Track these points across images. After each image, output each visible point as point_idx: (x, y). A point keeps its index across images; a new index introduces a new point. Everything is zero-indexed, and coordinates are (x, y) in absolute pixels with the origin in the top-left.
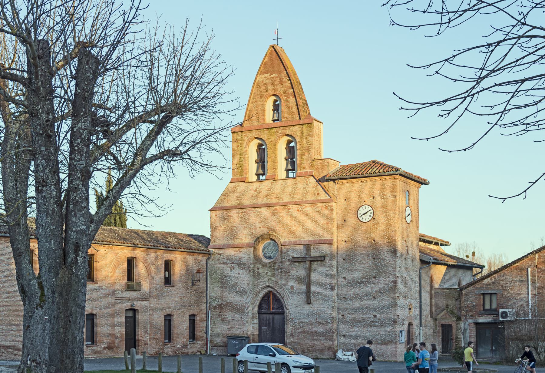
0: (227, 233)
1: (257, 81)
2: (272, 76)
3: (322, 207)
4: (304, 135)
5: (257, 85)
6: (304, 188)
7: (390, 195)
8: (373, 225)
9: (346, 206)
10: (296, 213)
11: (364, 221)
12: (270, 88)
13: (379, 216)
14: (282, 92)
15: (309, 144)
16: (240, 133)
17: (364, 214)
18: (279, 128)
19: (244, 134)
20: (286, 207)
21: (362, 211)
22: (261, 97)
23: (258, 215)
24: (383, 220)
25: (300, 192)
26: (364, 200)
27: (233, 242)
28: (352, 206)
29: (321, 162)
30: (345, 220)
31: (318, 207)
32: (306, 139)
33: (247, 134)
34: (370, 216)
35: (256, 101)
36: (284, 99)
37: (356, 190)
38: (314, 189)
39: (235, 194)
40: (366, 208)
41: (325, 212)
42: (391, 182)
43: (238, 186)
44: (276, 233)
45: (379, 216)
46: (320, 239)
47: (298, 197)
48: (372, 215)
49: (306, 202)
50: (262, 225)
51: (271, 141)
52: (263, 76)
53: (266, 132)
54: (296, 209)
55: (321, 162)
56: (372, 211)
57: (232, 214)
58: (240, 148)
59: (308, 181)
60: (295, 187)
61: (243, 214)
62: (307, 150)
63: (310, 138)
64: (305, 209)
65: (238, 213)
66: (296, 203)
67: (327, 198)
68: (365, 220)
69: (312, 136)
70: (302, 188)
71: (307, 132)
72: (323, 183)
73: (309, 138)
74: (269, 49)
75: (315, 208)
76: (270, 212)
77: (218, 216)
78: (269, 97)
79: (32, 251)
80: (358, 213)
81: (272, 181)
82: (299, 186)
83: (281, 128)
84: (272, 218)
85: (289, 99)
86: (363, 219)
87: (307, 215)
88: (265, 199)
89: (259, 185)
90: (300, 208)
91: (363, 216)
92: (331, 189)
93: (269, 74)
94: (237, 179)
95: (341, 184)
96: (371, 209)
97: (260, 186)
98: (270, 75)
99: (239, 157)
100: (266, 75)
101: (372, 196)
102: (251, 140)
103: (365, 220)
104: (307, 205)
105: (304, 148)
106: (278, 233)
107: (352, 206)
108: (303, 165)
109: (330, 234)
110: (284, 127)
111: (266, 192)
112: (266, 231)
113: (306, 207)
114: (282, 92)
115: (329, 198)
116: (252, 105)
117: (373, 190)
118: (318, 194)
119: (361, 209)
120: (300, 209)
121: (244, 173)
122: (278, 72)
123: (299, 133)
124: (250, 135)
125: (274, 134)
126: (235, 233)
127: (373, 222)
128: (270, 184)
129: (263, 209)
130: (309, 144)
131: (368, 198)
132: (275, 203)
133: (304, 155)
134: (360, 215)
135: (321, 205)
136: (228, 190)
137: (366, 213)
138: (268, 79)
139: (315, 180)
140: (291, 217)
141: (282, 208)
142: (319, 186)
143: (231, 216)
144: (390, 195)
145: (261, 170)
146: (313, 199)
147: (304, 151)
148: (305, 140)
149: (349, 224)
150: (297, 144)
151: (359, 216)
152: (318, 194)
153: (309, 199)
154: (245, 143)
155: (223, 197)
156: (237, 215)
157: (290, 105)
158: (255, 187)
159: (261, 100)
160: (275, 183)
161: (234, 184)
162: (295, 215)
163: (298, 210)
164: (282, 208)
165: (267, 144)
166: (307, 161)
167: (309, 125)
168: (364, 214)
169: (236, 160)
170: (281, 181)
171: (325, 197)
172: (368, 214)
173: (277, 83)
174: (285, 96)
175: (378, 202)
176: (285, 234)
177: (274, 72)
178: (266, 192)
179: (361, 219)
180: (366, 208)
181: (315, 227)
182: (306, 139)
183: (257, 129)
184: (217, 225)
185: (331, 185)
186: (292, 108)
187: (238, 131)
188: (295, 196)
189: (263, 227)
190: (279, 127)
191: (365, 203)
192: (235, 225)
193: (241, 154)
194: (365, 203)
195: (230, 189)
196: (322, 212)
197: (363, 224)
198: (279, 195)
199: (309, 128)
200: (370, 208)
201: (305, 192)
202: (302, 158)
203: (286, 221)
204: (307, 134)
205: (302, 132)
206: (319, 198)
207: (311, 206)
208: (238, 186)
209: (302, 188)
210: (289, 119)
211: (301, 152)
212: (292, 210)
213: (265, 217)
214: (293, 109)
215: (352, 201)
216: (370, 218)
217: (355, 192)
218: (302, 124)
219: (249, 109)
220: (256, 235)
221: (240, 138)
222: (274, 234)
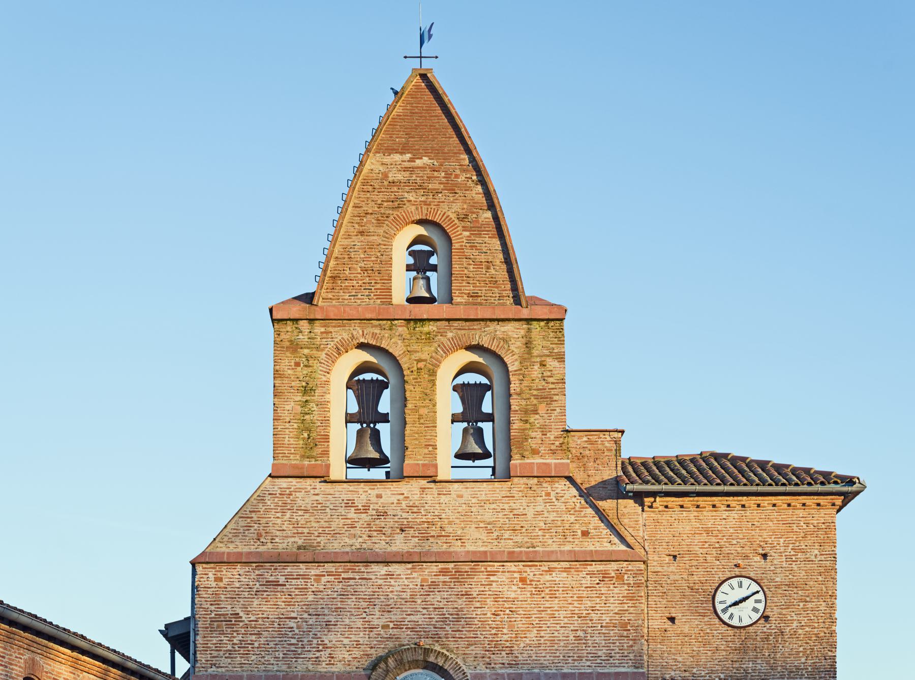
0: (262, 640)
1: (365, 170)
2: (418, 162)
3: (605, 576)
4: (535, 352)
5: (363, 184)
6: (539, 513)
7: (816, 552)
8: (762, 635)
9: (677, 577)
10: (515, 588)
11: (735, 622)
12: (411, 197)
13: (784, 612)
14: (453, 216)
15: (551, 380)
16: (304, 325)
17: (736, 604)
18: (446, 323)
19: (319, 329)
20: (481, 567)
21: (728, 594)
22: (379, 223)
23: (380, 587)
24: (795, 624)
25: (522, 524)
26: (735, 562)
27: (284, 668)
28: (695, 578)
29: (593, 438)
30: (672, 620)
31: (591, 574)
32: (543, 365)
33: (331, 329)
34: (755, 610)
35: (362, 233)
36: (460, 237)
37: (708, 532)
38: (572, 519)
39: (288, 515)
40: (740, 586)
41: (616, 591)
42: (820, 516)
43: (299, 490)
44: (443, 646)
45: (784, 612)
46: (600, 670)
47: (519, 539)
48: (761, 606)
49: (549, 558)
50: (394, 618)
51: (419, 361)
52: (387, 159)
53: (402, 330)
54: (516, 575)
55: (593, 438)
56: (760, 596)
57: (282, 580)
58: (301, 371)
59: (553, 494)
60: (506, 506)
61: (324, 579)
62: (547, 398)
63: (556, 363)
64: (548, 577)
65: (305, 577)
66: (513, 558)
67: (614, 548)
68: (740, 620)
69: (561, 358)
70: (530, 512)
71: (545, 343)
72: (598, 502)
73: (552, 363)
74: (408, 81)
75: (583, 574)
76: (423, 580)
77: (225, 581)
78: (407, 224)
79: (377, 379)
80: (718, 599)
81: (423, 482)
82: (520, 504)
83: (456, 324)
84: (429, 598)
85: (479, 240)
86: (731, 617)
87: (553, 596)
88: (399, 538)
89: (376, 492)
90: (530, 573)
91: (731, 610)
92: (625, 521)
93: (408, 156)
94: (295, 467)
95: (661, 508)
96: (758, 588)
97: (379, 496)
98: (412, 160)
99: (299, 398)
100: (397, 157)
101: (761, 552)
102: (341, 350)
103: (740, 620)
104: (555, 565)
105: (535, 393)
106: (452, 645)
107: (695, 578)
108: (532, 443)
109: (631, 656)
110: (466, 320)
111: (405, 515)
112: (406, 637)
113: (550, 570)
114: (453, 216)
115: (623, 547)
116: (346, 242)
117: (765, 534)
118: (585, 534)
119: (725, 587)
120: (531, 577)
121: (317, 451)
122: (435, 153)
123: (517, 346)
124: (341, 334)
125: (429, 338)
126: (293, 641)
127: (762, 627)
128: (417, 491)
129: (395, 568)
130: (551, 380)
131: (746, 557)
132: (438, 553)
133: (535, 412)
134: (724, 606)
135: (601, 567)
136: (261, 499)
137: (745, 599)
138: (406, 169)
139: (574, 492)
140: (496, 598)
141: (467, 568)
142: (590, 511)
143: (276, 584)
144: (816, 552)
145: (371, 448)
146: (568, 548)
147: (535, 402)
148: (536, 367)
149: (686, 630)
150: (512, 378)
151: (719, 607)
152: (585, 534)
153: (554, 547)
154: (323, 355)
155: (242, 523)
156: (301, 582)
157: (483, 258)
158: (364, 497)
159: (381, 231)
160: (435, 492)
161: (283, 483)
162: (513, 595)
163: (523, 580)
164: (467, 568)
165: (405, 366)
166: (544, 430)
167: (551, 324)
168: (736, 604)
169: (287, 407)
170: (456, 485)
171: (606, 543)
172: (750, 603)
173: (437, 186)
174: (465, 229)
175: (779, 570)
176: (478, 650)
177: (426, 154)
178: (405, 515)
179: (725, 617)
180: (740, 586)
181: (580, 633)
182: (543, 365)
183: (368, 316)
184: (223, 611)
185: (625, 510)
186: (488, 268)
187: (297, 316)
188: (506, 536)
189: (397, 627)
190: (448, 320)
191: (737, 571)
192: (293, 615)
193: (307, 390)
194: (737, 571)
195: (268, 497)
196: (604, 590)
197: (731, 632)
198: (449, 529)
199: (552, 335)
200: (755, 587)
201: (542, 524)
202: (526, 421)
203: (479, 611)
204: (546, 352)
205: (528, 344)
206: (590, 546)
207: (566, 570)
208: (299, 490)
209: (530, 512)
210: (479, 300)
211: (524, 403)
212: (502, 578)
213: (404, 595)
214: (492, 271)
215: (695, 563)
216: (756, 616)
217: (704, 537)
218: (528, 321)
219: (336, 253)
220: (373, 651)
221: (303, 338)
222: (437, 648)
